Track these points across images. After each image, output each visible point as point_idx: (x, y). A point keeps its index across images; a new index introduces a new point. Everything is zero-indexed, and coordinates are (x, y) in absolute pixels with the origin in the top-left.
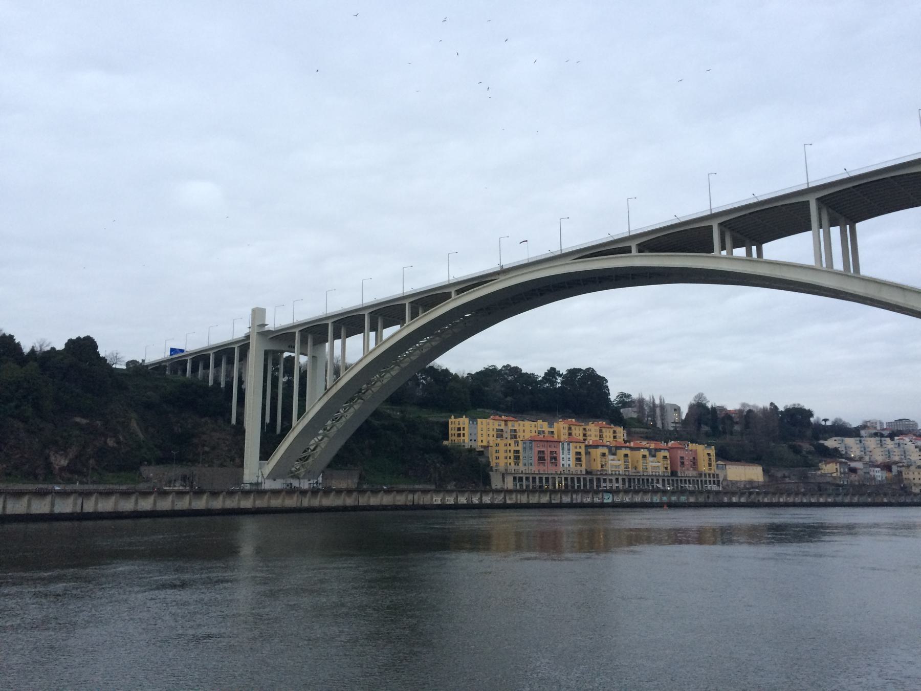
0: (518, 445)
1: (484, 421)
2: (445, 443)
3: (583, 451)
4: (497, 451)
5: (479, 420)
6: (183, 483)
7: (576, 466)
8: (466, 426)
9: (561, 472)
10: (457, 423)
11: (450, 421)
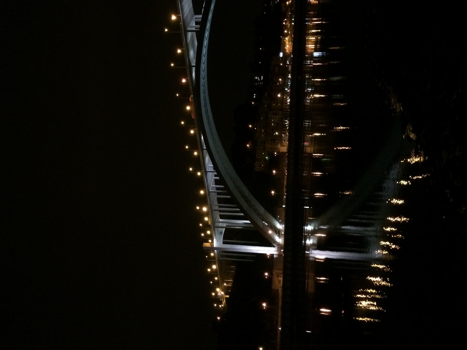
4: (271, 149)
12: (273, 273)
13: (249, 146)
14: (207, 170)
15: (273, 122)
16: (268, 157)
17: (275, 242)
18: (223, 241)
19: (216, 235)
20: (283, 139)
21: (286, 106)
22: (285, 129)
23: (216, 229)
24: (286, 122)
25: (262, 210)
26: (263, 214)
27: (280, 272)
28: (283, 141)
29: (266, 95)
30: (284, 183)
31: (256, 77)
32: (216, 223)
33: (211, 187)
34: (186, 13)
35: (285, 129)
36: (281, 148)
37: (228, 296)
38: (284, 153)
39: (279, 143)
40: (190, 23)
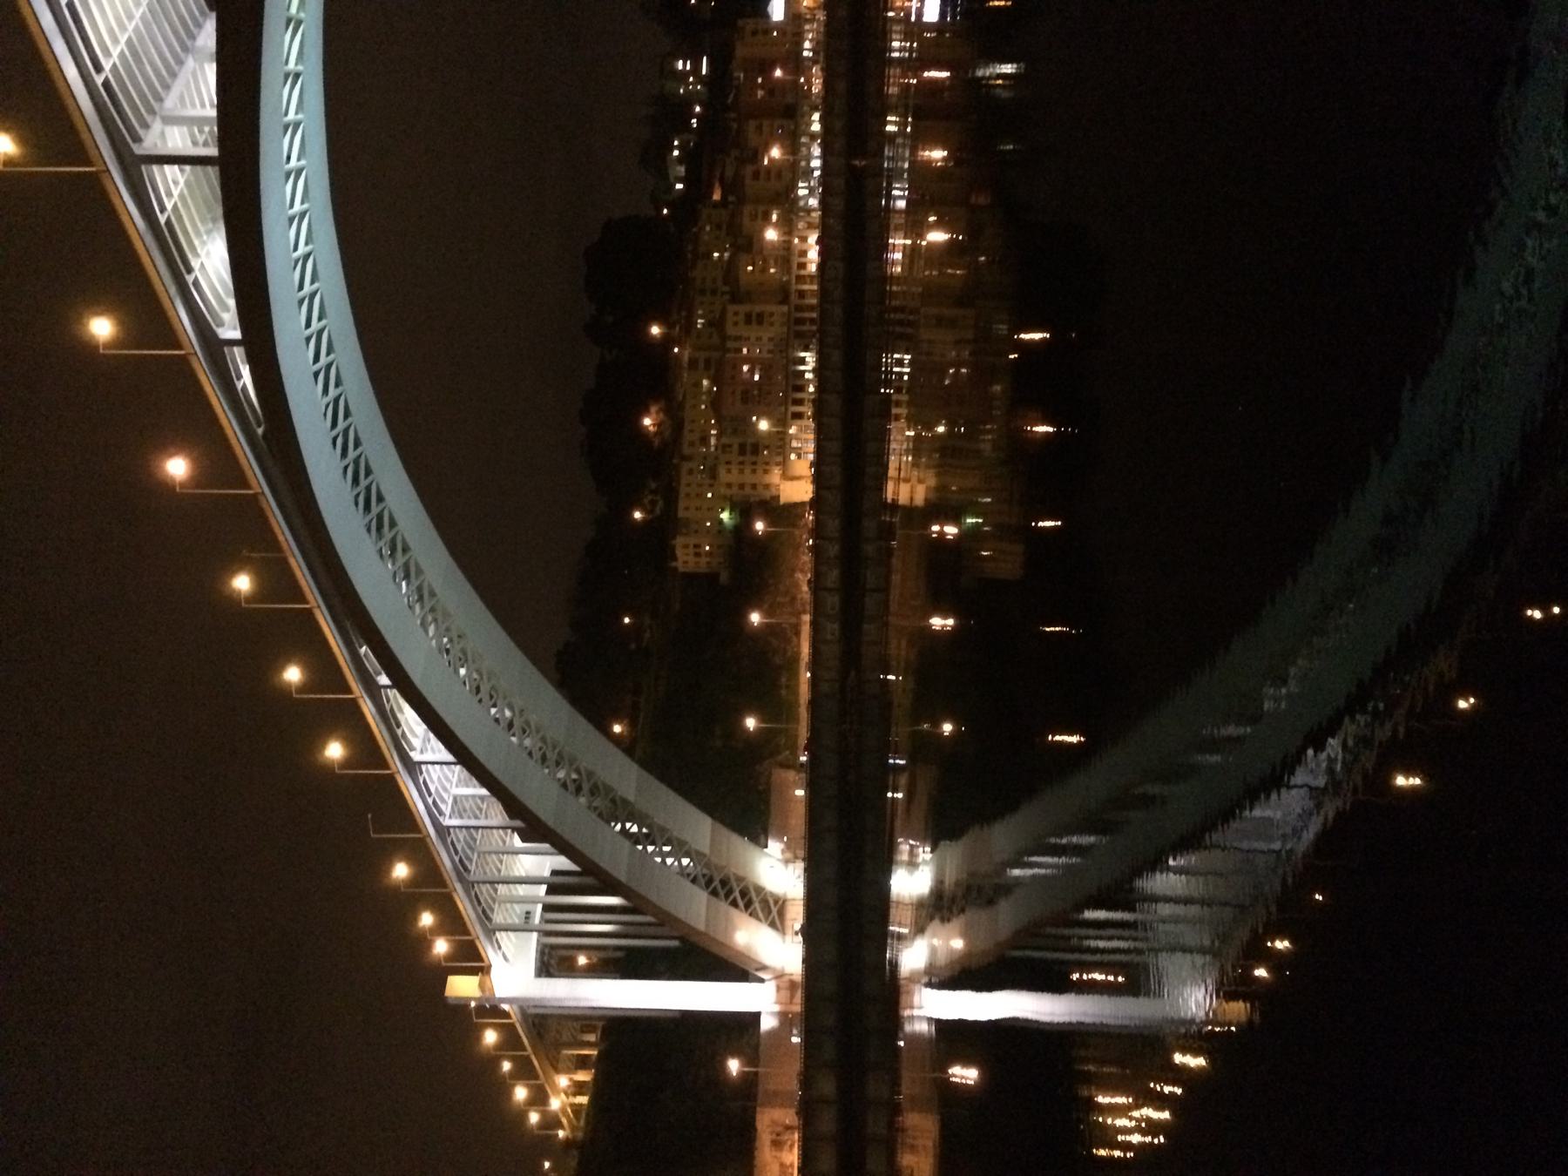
0: (730, 446)
1: (682, 504)
2: (724, 577)
3: (743, 309)
4: (742, 486)
5: (681, 514)
6: (787, 1147)
7: (772, 324)
8: (692, 541)
9: (783, 358)
10: (685, 558)
11: (681, 569)
12: (759, 1126)
13: (654, 425)
15: (746, 360)
16: (730, 514)
17: (764, 968)
18: (538, 941)
20: (794, 444)
21: (801, 279)
22: (799, 395)
23: (497, 934)
24: (803, 361)
25: (700, 828)
26: (707, 851)
27: (787, 1122)
28: (793, 456)
29: (717, 196)
30: (799, 645)
31: (681, 62)
32: (496, 907)
33: (450, 802)
34: (123, 39)
35: (799, 395)
36: (782, 487)
37: (583, 1100)
38: (794, 509)
39: (778, 464)
40: (167, 87)
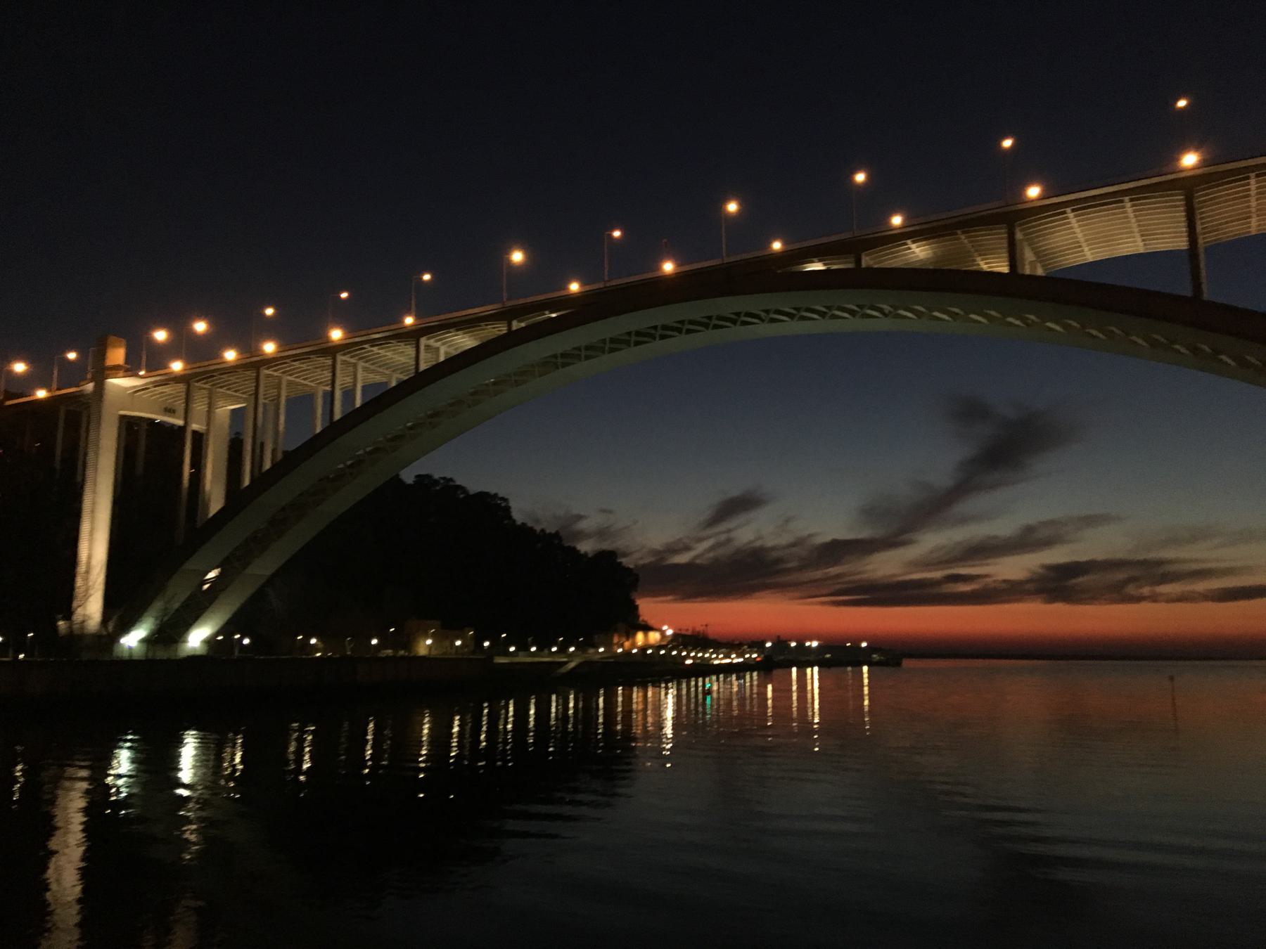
14: (423, 341)
19: (160, 389)
33: (353, 360)
